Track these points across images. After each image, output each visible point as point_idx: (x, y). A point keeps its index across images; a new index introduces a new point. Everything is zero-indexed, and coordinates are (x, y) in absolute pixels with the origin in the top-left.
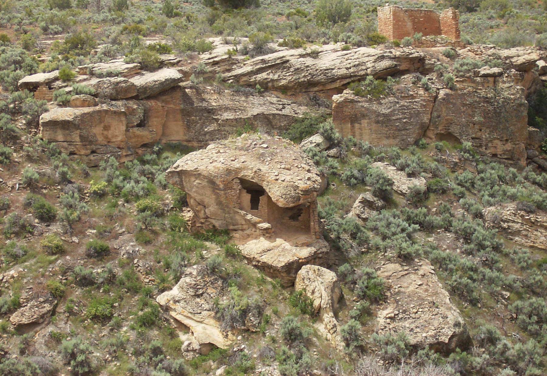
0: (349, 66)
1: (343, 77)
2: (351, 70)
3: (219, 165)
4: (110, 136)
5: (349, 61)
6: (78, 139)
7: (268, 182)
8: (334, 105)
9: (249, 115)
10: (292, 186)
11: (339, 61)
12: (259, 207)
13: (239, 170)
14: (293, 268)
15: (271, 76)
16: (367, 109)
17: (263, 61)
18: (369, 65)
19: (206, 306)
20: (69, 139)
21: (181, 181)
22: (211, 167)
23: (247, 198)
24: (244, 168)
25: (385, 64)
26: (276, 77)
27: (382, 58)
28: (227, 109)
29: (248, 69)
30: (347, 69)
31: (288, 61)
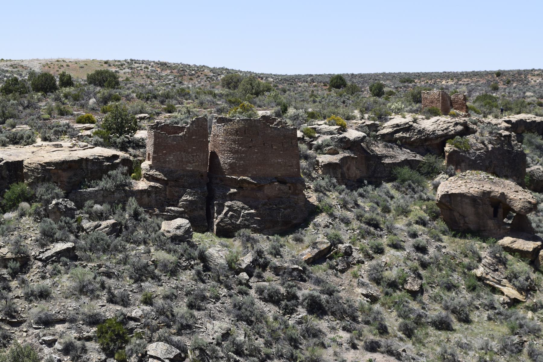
0: (442, 129)
1: (441, 136)
2: (445, 131)
3: (477, 190)
4: (350, 173)
5: (441, 126)
6: (340, 176)
7: (510, 199)
8: (447, 154)
9: (399, 161)
10: (527, 202)
11: (436, 126)
12: (498, 216)
13: (489, 193)
14: (536, 251)
15: (404, 135)
16: (464, 156)
17: (397, 125)
18: (451, 128)
19: (503, 276)
20: (336, 176)
21: (451, 200)
22: (471, 191)
23: (491, 210)
24: (493, 191)
25: (460, 128)
26: (408, 136)
27: (456, 124)
28: (386, 157)
29: (390, 130)
30: (443, 131)
31: (412, 126)
